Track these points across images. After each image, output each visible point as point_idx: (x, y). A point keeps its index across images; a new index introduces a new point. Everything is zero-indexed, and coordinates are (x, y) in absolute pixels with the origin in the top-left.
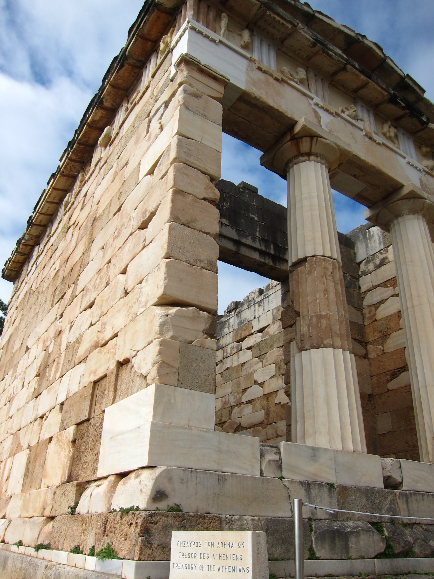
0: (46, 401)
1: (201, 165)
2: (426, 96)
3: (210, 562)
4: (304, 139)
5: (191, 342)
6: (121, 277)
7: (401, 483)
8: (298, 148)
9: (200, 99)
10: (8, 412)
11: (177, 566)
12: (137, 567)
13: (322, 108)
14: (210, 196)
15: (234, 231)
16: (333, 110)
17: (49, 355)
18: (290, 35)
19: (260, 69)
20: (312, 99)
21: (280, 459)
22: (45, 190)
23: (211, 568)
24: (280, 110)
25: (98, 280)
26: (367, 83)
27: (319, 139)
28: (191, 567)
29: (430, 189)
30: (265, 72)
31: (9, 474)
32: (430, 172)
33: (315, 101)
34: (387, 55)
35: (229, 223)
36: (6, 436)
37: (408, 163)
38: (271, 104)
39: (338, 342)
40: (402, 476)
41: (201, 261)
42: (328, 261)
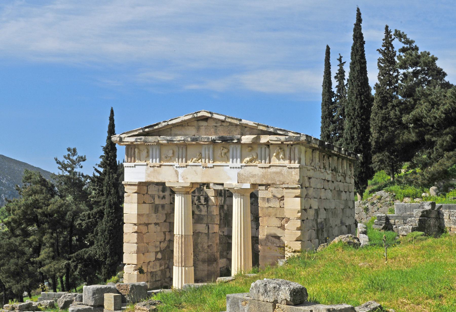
9: (130, 197)
13: (179, 167)
14: (134, 231)
16: (184, 164)
19: (151, 167)
20: (174, 165)
24: (160, 181)
29: (245, 176)
32: (247, 164)
33: (176, 166)
37: (231, 168)
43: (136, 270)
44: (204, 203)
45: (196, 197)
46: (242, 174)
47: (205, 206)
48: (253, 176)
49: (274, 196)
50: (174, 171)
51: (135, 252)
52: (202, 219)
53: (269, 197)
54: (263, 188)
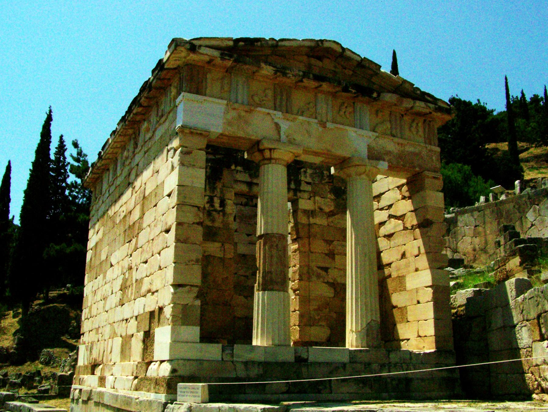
0: (127, 311)
1: (191, 202)
2: (382, 70)
3: (189, 394)
4: (266, 151)
5: (187, 304)
6: (158, 255)
7: (308, 359)
8: (263, 156)
10: (104, 307)
11: (179, 395)
12: (165, 396)
15: (247, 175)
17: (127, 279)
18: (257, 71)
21: (233, 353)
22: (108, 140)
23: (190, 396)
25: (148, 249)
26: (321, 85)
27: (275, 150)
28: (183, 396)
29: (376, 151)
30: (238, 110)
31: (112, 349)
34: (345, 47)
35: (243, 169)
36: (105, 323)
38: (241, 134)
39: (276, 287)
40: (308, 356)
41: (192, 260)
42: (276, 237)
43: (197, 297)
44: (219, 209)
45: (207, 198)
46: (373, 148)
47: (221, 213)
48: (389, 153)
49: (321, 209)
50: (273, 125)
51: (197, 261)
52: (215, 234)
53: (312, 208)
54: (306, 195)
